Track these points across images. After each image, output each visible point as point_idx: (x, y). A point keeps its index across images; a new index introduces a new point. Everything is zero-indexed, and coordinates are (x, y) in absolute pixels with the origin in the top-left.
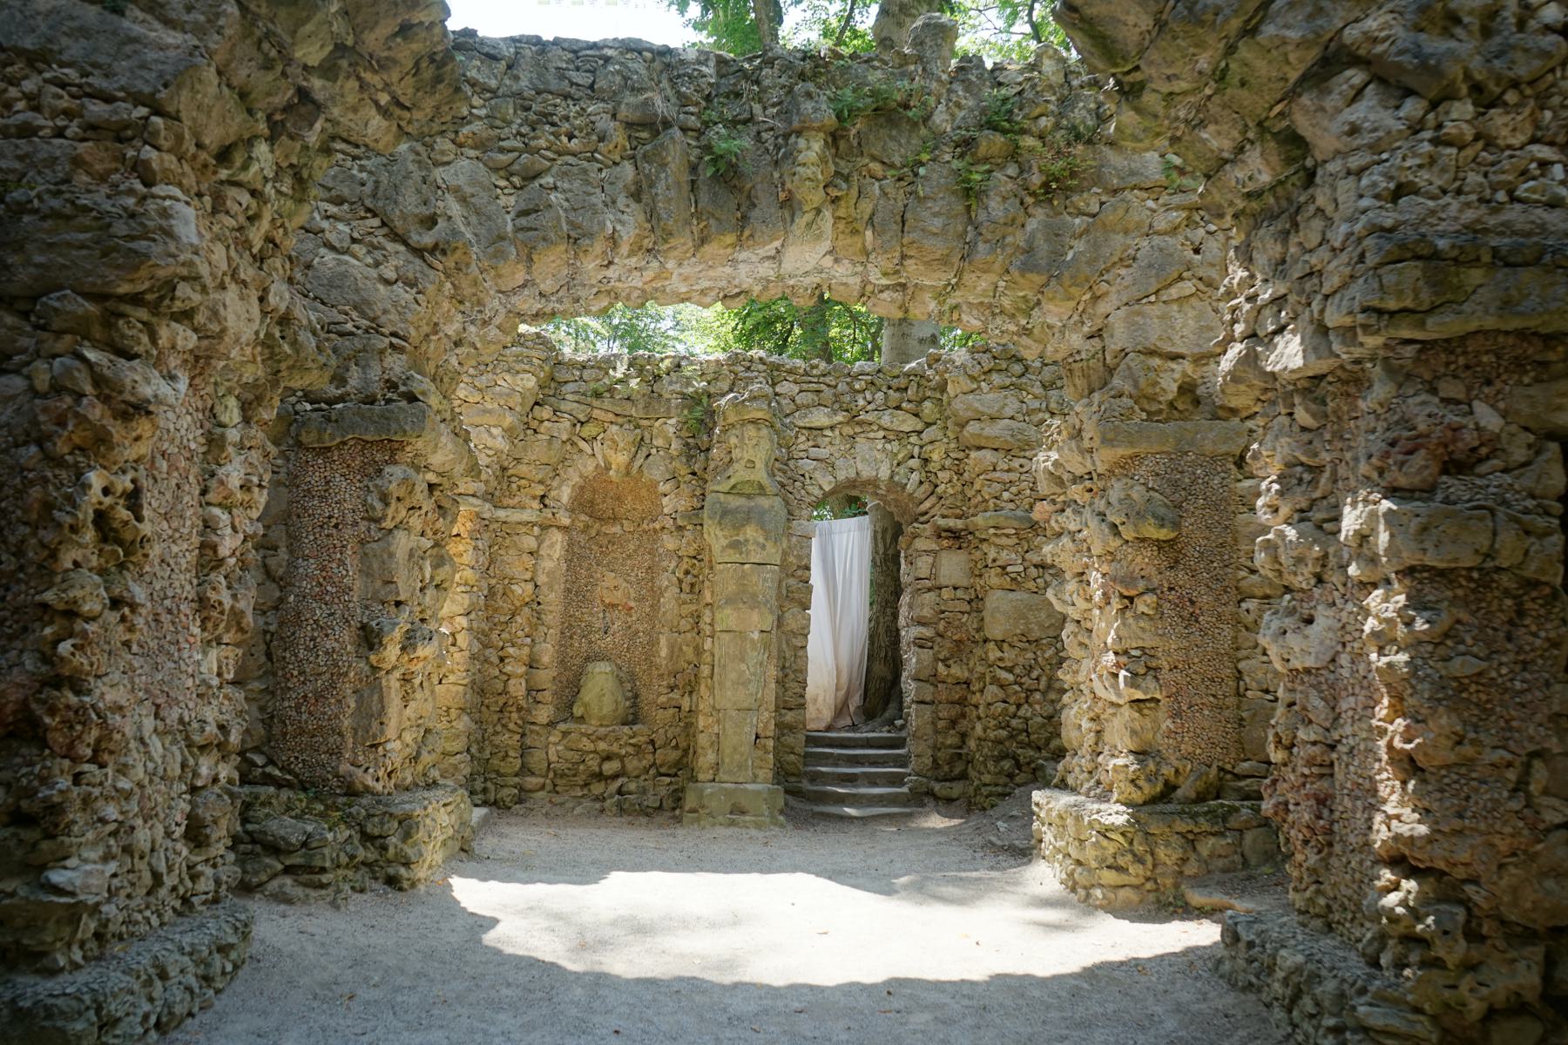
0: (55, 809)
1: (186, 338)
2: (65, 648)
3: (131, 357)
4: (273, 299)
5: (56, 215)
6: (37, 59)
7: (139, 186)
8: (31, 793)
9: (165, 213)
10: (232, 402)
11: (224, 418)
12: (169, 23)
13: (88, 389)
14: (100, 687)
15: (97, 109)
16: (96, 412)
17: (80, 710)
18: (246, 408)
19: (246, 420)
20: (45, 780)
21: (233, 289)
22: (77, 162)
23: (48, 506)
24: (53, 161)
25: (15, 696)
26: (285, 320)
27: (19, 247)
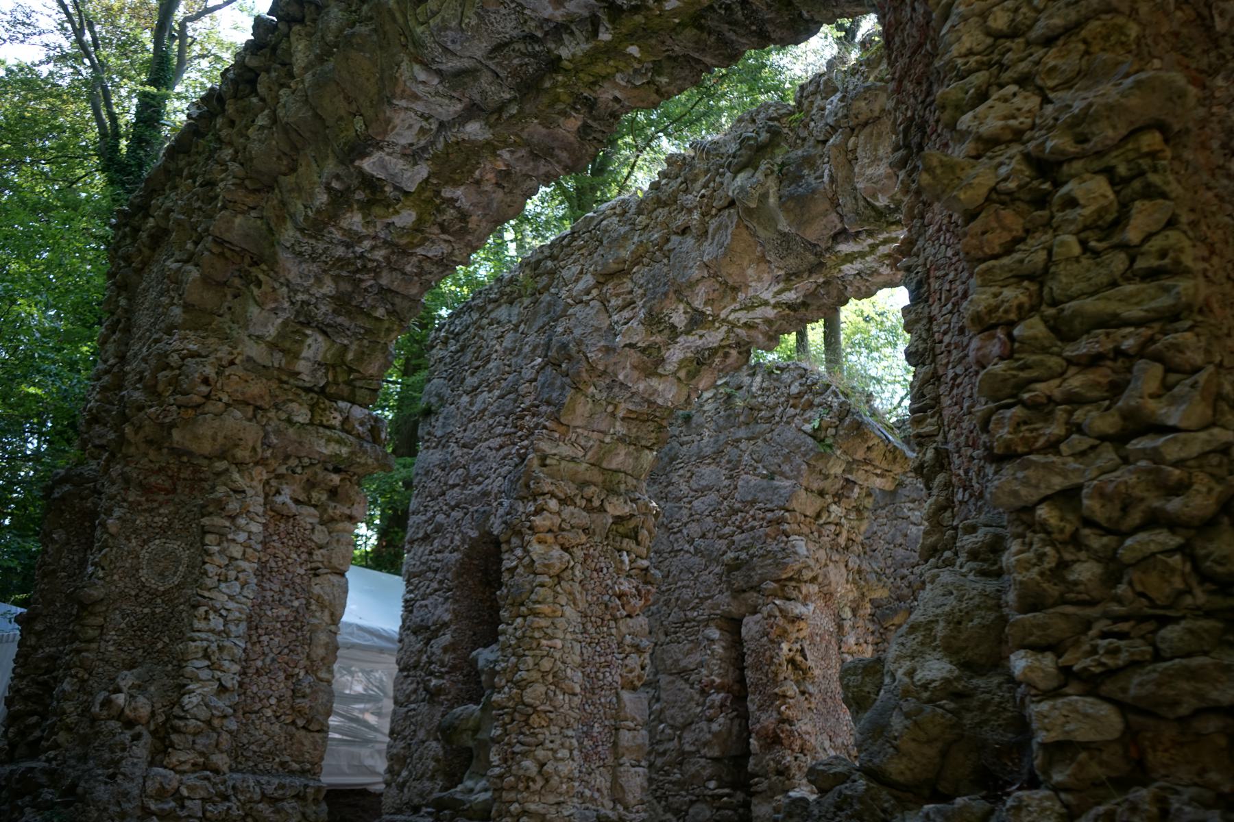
0: (788, 768)
1: (814, 588)
2: (783, 708)
3: (789, 599)
4: (850, 565)
5: (762, 556)
6: (753, 502)
7: (785, 539)
8: (779, 762)
9: (793, 546)
10: (847, 609)
11: (844, 616)
12: (787, 478)
13: (777, 614)
14: (798, 725)
15: (769, 515)
16: (781, 621)
17: (792, 731)
18: (854, 612)
19: (854, 616)
20: (783, 757)
21: (831, 565)
22: (767, 535)
23: (772, 657)
24: (760, 537)
25: (772, 727)
26: (859, 572)
27: (754, 569)
